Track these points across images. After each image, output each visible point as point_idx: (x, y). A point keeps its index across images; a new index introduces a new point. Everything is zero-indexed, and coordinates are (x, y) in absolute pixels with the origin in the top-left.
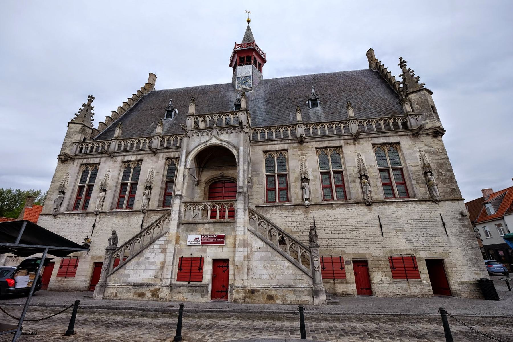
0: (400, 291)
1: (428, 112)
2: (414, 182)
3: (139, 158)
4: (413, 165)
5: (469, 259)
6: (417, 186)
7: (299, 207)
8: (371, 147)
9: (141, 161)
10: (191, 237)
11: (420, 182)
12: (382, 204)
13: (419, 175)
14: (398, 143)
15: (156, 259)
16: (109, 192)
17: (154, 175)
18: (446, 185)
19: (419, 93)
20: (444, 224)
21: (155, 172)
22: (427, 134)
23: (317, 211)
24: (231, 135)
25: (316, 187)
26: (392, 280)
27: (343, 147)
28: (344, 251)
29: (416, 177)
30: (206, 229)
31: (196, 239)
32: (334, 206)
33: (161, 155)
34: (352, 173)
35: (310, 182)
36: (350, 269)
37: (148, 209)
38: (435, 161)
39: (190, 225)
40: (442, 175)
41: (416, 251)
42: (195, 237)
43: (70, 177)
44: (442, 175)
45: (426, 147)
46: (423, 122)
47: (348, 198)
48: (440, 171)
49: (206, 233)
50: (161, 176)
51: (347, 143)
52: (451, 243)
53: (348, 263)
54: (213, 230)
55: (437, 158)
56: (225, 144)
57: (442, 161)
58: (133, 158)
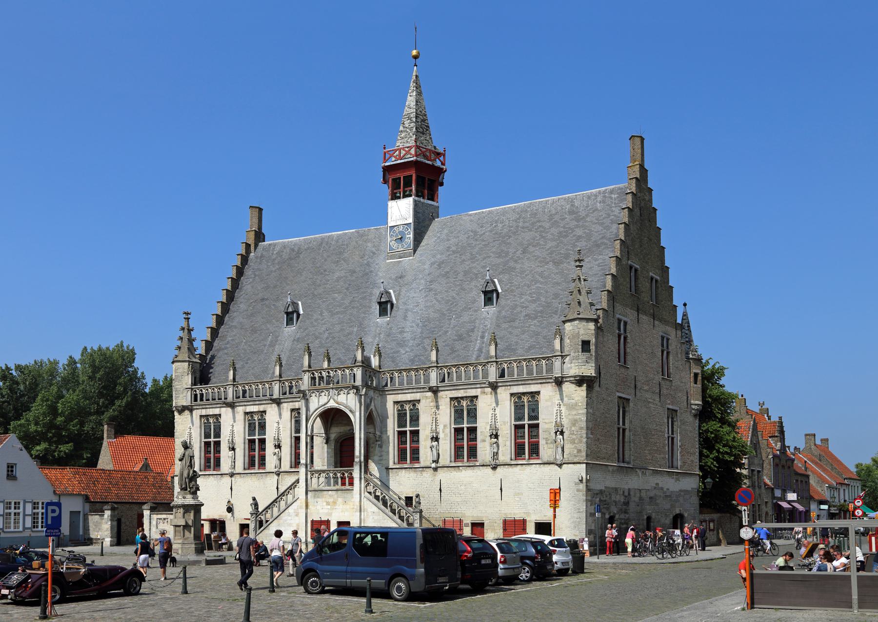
3: (262, 408)
4: (547, 421)
6: (546, 446)
14: (538, 393)
15: (292, 522)
25: (446, 446)
38: (570, 417)
41: (528, 514)
48: (573, 428)
50: (289, 432)
53: (467, 525)
55: (574, 412)
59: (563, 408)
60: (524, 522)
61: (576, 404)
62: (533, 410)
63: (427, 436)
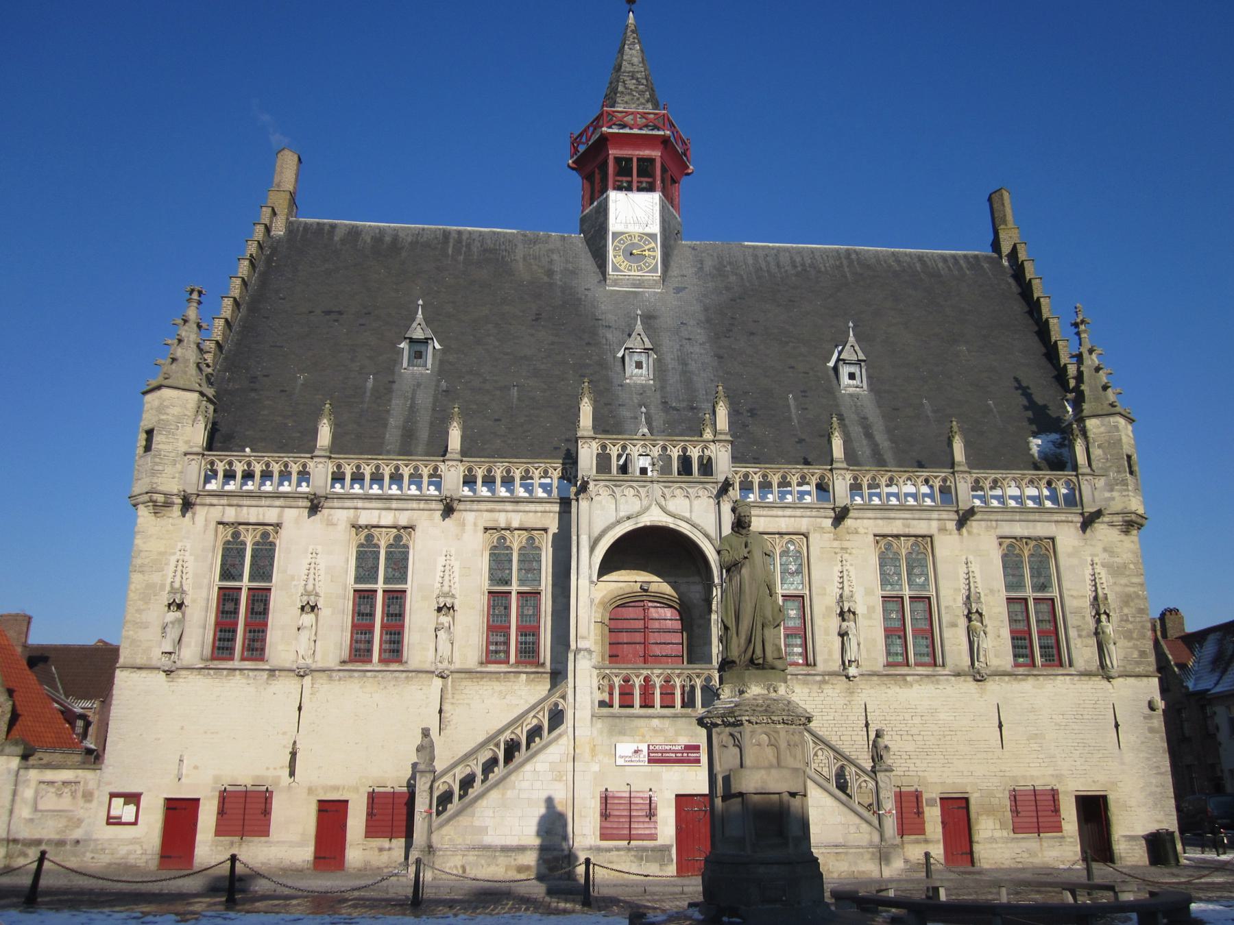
0: (1025, 855)
1: (1119, 472)
2: (1073, 633)
3: (403, 519)
4: (1075, 593)
5: (1151, 794)
6: (1078, 641)
7: (834, 680)
8: (996, 542)
9: (410, 528)
10: (625, 748)
11: (1084, 633)
12: (1007, 678)
13: (1084, 617)
16: (325, 612)
17: (456, 574)
18: (1130, 644)
19: (1107, 419)
20: (1117, 726)
21: (457, 566)
22: (1111, 524)
23: (872, 691)
24: (696, 503)
26: (1012, 835)
27: (936, 539)
28: (925, 777)
29: (1079, 623)
30: (655, 730)
31: (636, 752)
32: (909, 678)
33: (470, 517)
34: (951, 603)
35: (860, 619)
36: (933, 815)
37: (452, 667)
38: (1118, 589)
39: (617, 720)
40: (1127, 620)
41: (1059, 777)
42: (634, 747)
43: (188, 557)
44: (1127, 620)
45: (1106, 555)
46: (1107, 495)
47: (939, 661)
48: (1126, 611)
49: (659, 742)
51: (942, 530)
52: (1123, 764)
53: (931, 803)
54: (671, 732)
55: (1123, 581)
56: (685, 528)
57: (1132, 590)
58: (387, 518)
59: (1103, 574)
60: (1054, 794)
61: (1125, 566)
62: (1039, 575)
63: (828, 608)
